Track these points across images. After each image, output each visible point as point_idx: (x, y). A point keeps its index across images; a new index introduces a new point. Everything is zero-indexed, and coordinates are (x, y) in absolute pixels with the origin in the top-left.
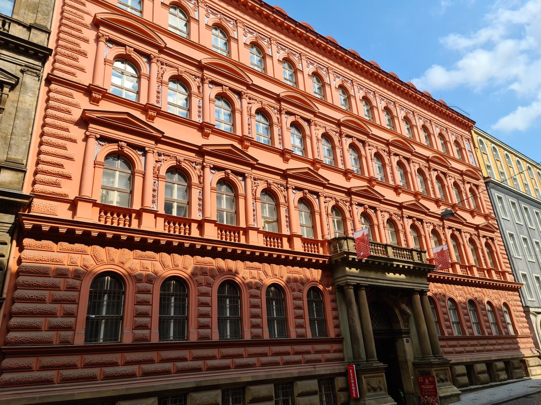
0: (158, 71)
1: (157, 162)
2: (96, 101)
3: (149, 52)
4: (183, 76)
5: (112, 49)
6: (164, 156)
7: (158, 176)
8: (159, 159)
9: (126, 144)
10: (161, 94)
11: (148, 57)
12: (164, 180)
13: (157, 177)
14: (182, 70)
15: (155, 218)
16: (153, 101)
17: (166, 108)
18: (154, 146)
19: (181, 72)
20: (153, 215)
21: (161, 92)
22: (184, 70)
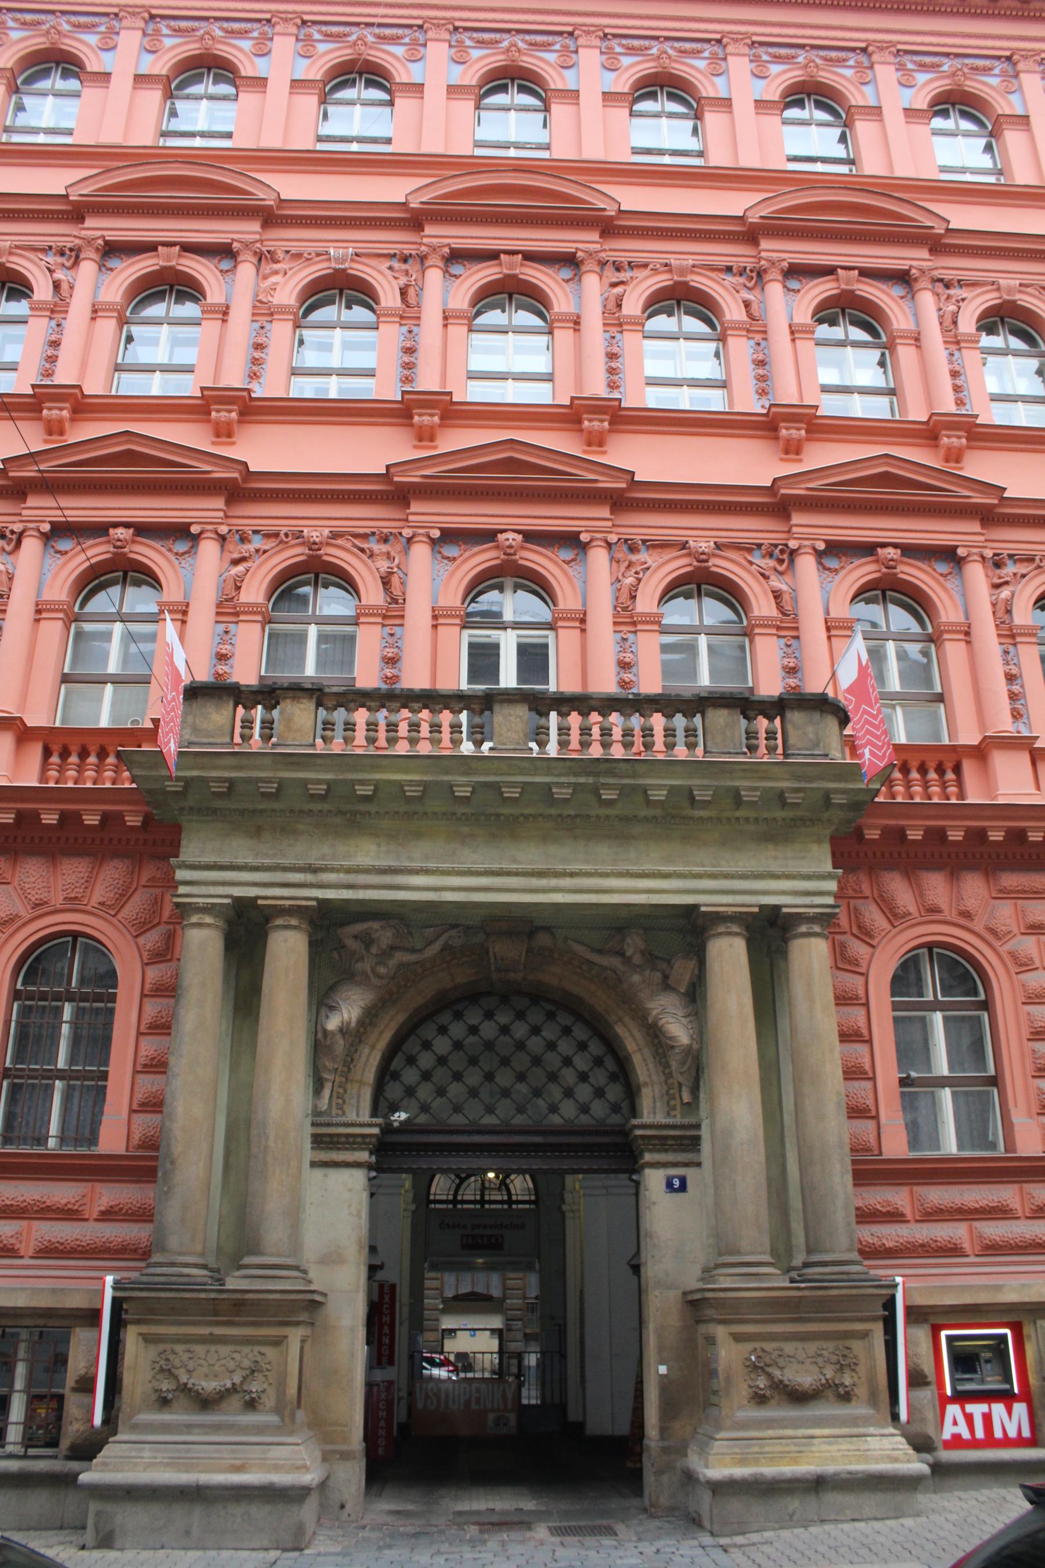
0: (940, 309)
1: (996, 586)
2: (792, 450)
3: (903, 265)
4: (1019, 302)
5: (802, 292)
6: (1015, 561)
7: (1011, 629)
8: (1000, 578)
9: (899, 551)
10: (962, 377)
11: (902, 278)
12: (1033, 640)
13: (1009, 634)
14: (1012, 282)
15: (1034, 763)
16: (948, 405)
17: (999, 415)
18: (982, 538)
19: (1010, 291)
20: (1025, 758)
21: (962, 371)
22: (1018, 282)
